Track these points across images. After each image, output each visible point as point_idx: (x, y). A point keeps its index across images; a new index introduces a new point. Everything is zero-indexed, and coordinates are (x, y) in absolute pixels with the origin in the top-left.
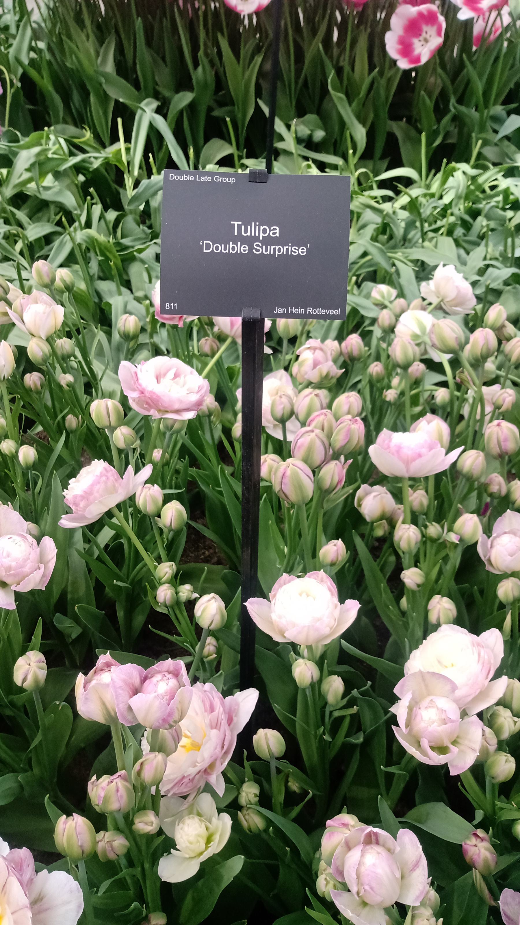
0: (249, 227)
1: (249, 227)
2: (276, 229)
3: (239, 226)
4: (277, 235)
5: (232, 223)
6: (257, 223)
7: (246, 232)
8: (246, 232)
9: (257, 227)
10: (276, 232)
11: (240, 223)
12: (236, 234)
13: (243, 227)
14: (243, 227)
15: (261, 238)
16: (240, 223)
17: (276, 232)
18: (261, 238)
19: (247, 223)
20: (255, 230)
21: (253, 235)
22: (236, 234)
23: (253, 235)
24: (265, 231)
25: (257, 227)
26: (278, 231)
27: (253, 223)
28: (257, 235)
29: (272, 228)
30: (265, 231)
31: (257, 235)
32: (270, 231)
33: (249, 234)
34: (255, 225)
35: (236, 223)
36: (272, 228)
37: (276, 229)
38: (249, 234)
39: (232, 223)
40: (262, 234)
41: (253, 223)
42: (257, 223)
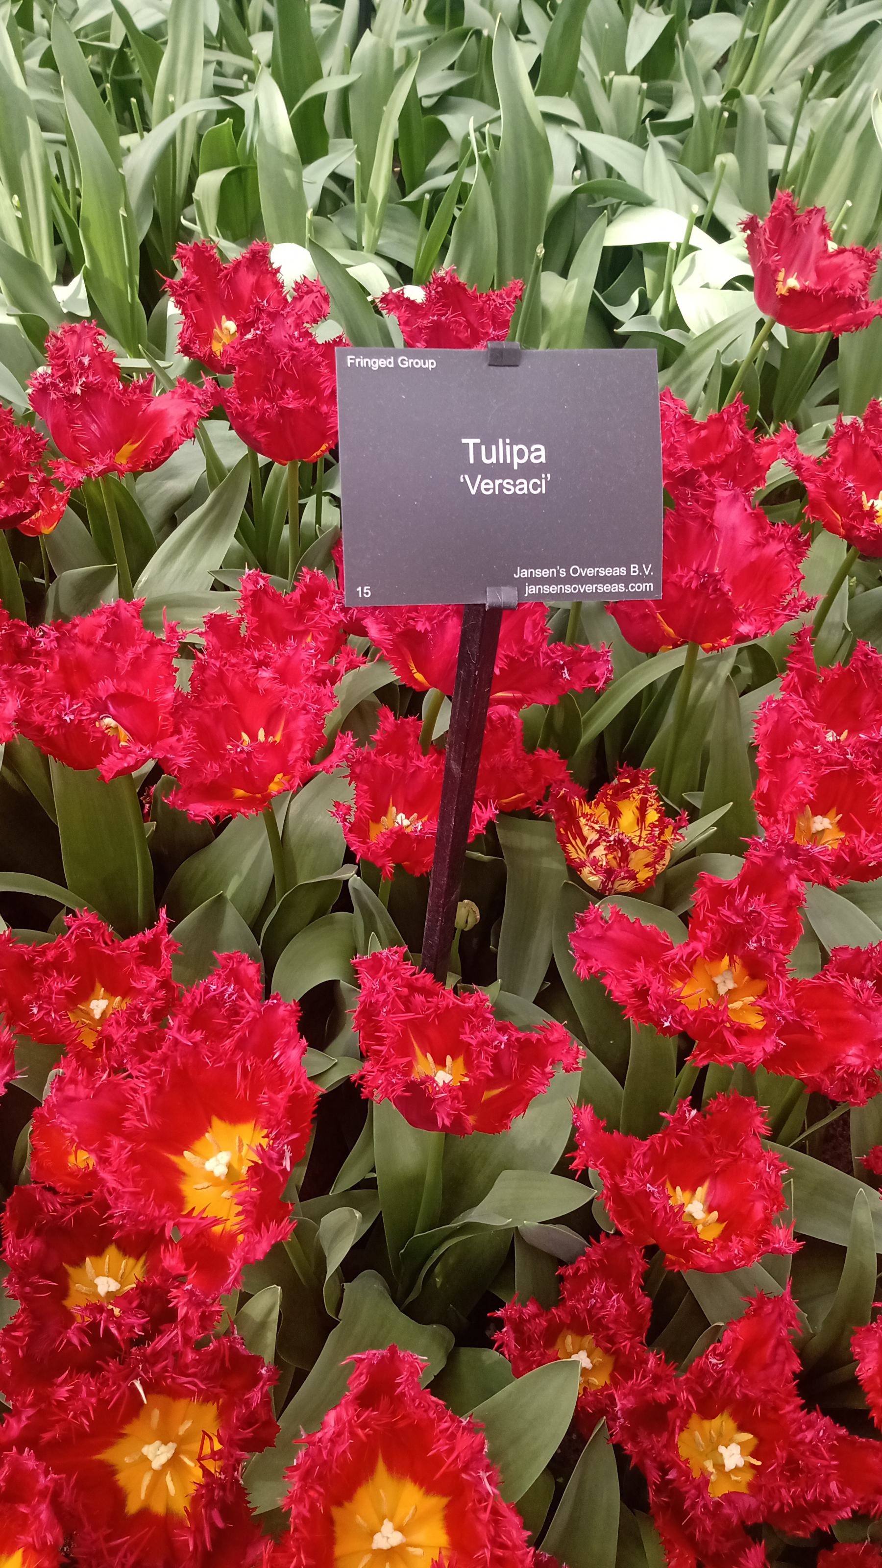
0: (494, 447)
1: (494, 447)
2: (539, 450)
3: (477, 447)
4: (543, 460)
5: (464, 441)
6: (508, 441)
7: (489, 456)
8: (489, 456)
9: (508, 447)
10: (539, 454)
11: (478, 441)
12: (472, 461)
13: (483, 448)
14: (483, 448)
15: (516, 467)
16: (478, 441)
17: (539, 454)
18: (516, 467)
19: (489, 441)
20: (503, 452)
21: (501, 461)
22: (472, 461)
23: (501, 461)
24: (521, 454)
25: (508, 447)
26: (543, 453)
27: (501, 441)
28: (508, 461)
29: (532, 449)
30: (521, 454)
31: (508, 461)
32: (530, 453)
33: (493, 460)
34: (505, 444)
35: (471, 442)
36: (532, 449)
37: (539, 450)
39: (464, 441)
40: (516, 461)
41: (501, 441)
42: (508, 441)
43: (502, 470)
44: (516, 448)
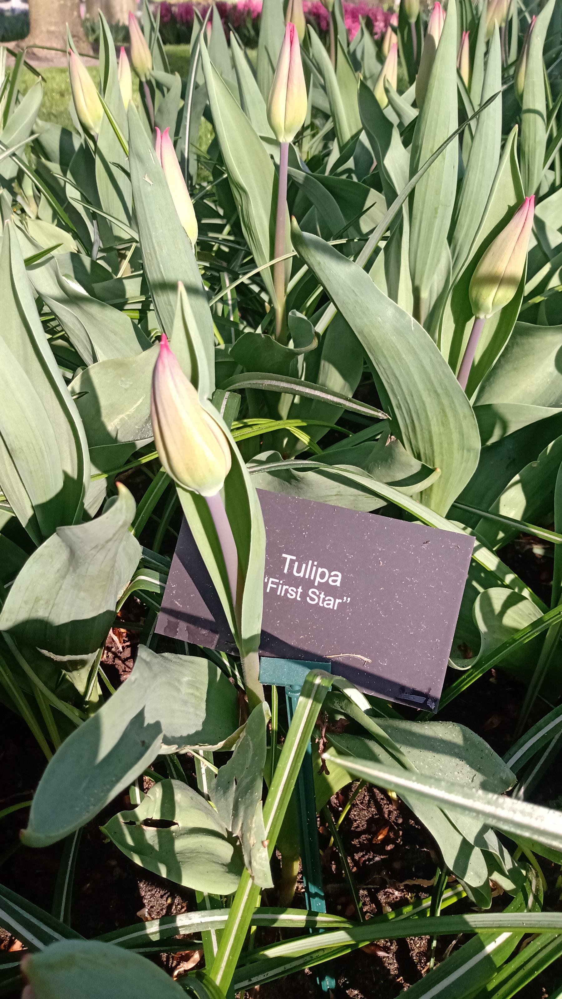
0: (304, 565)
1: (304, 565)
2: (337, 576)
3: (292, 562)
4: (338, 584)
5: (284, 555)
6: (316, 563)
7: (299, 571)
8: (299, 571)
9: (314, 568)
11: (294, 558)
12: (286, 571)
13: (296, 563)
14: (296, 563)
15: (316, 584)
16: (294, 558)
18: (316, 584)
19: (301, 561)
21: (307, 577)
22: (286, 571)
23: (307, 577)
24: (322, 575)
25: (314, 568)
26: (339, 579)
27: (310, 562)
28: (312, 578)
29: (332, 574)
30: (322, 575)
31: (312, 578)
32: (330, 576)
33: (301, 575)
34: (313, 565)
35: (289, 557)
38: (301, 575)
39: (284, 555)
40: (318, 579)
41: (310, 562)
42: (316, 563)
43: (308, 584)
44: (320, 570)
